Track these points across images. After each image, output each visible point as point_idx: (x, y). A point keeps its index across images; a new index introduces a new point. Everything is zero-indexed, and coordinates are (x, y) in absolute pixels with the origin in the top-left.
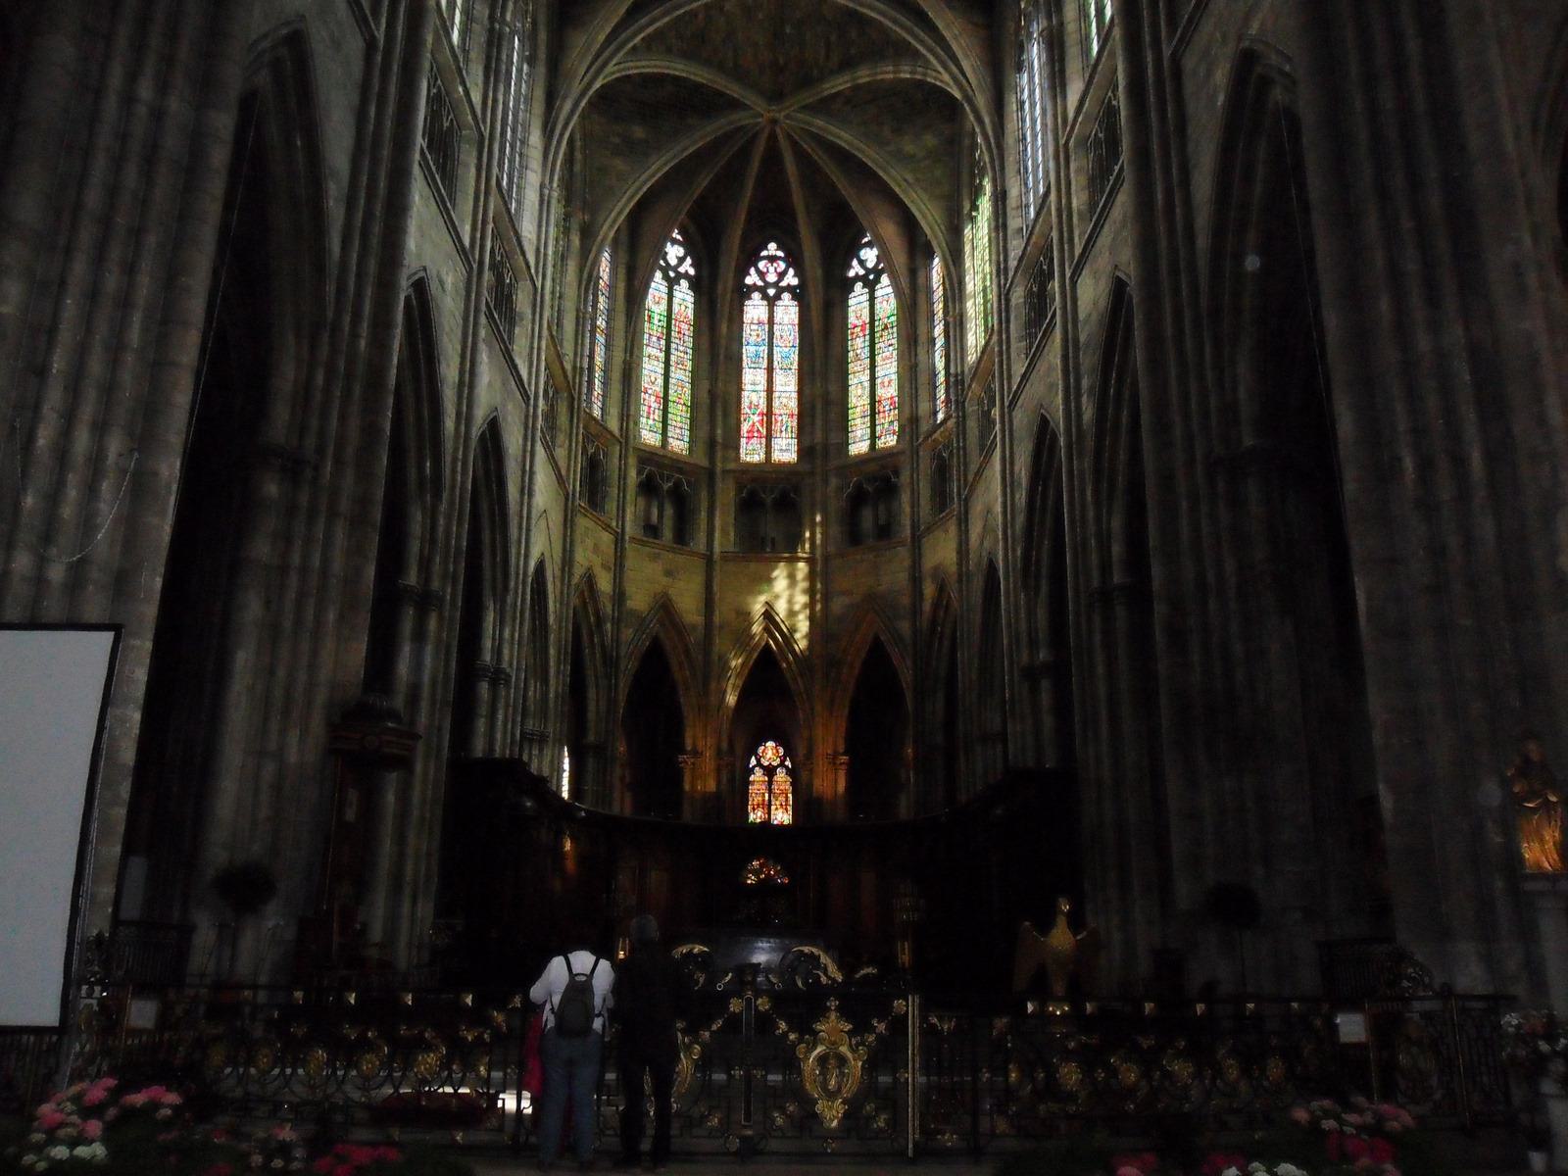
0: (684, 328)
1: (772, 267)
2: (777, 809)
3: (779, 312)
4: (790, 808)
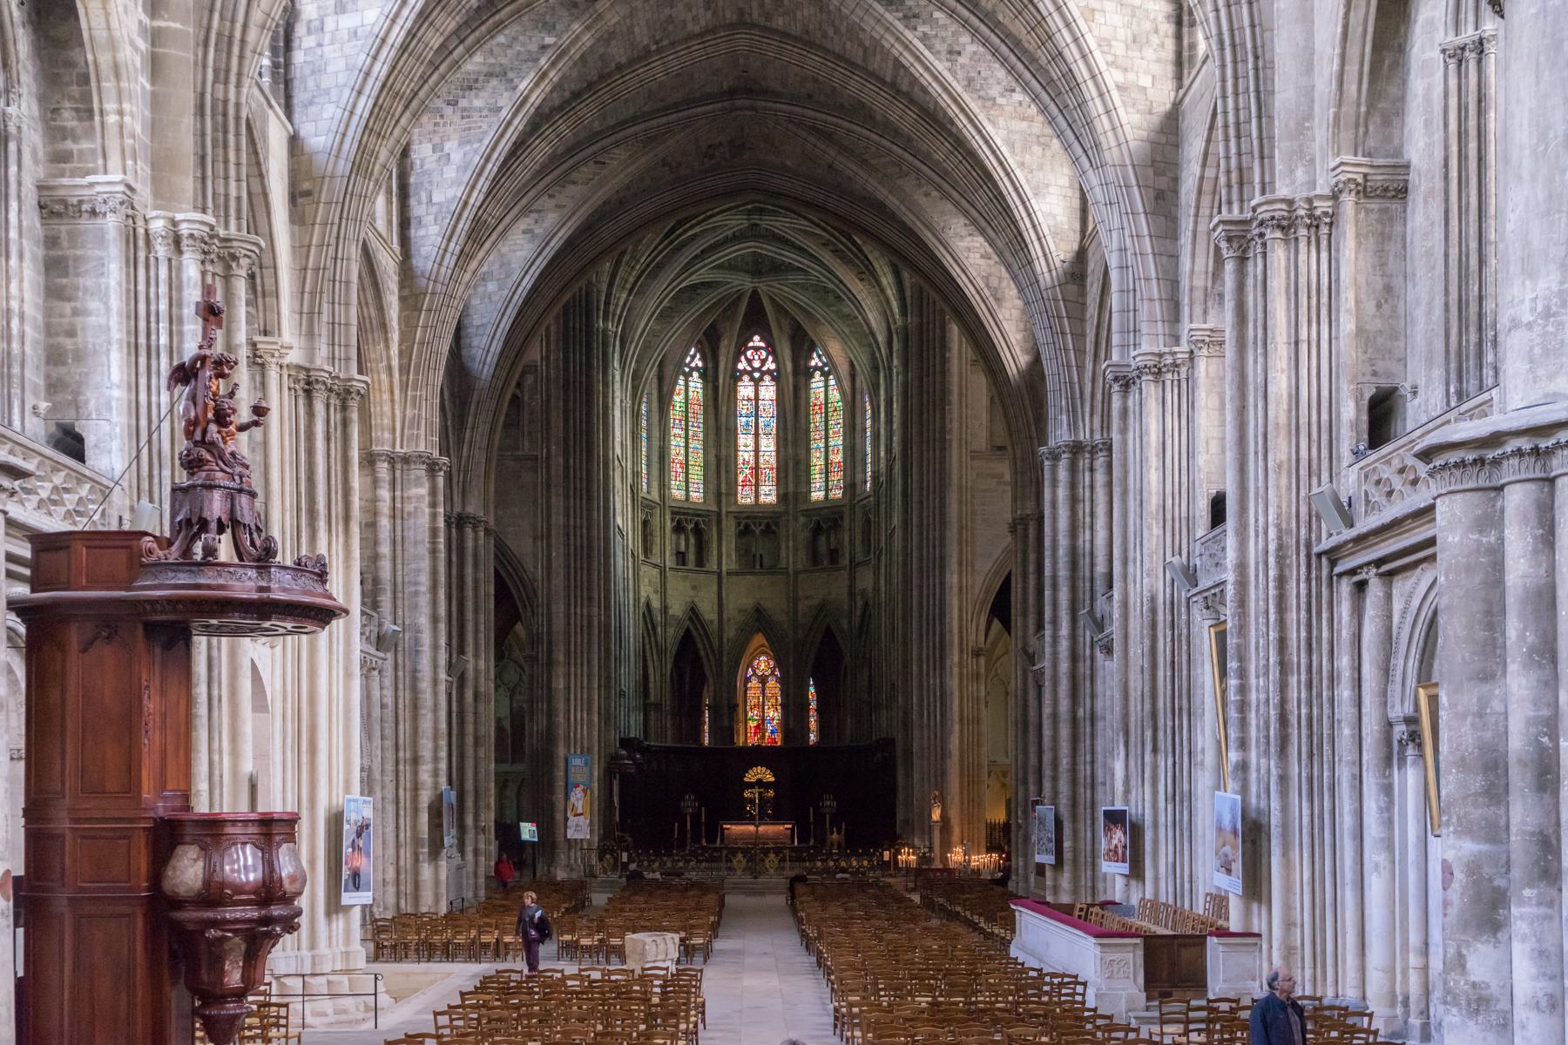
0: (697, 409)
1: (757, 355)
3: (763, 393)
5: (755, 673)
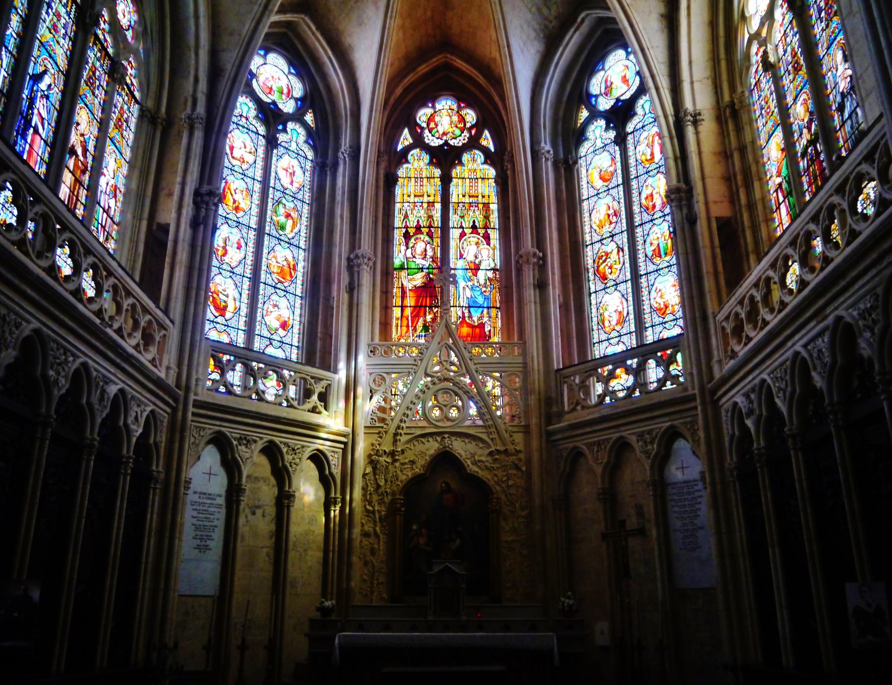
2: (463, 235)
4: (494, 235)
5: (419, 142)
